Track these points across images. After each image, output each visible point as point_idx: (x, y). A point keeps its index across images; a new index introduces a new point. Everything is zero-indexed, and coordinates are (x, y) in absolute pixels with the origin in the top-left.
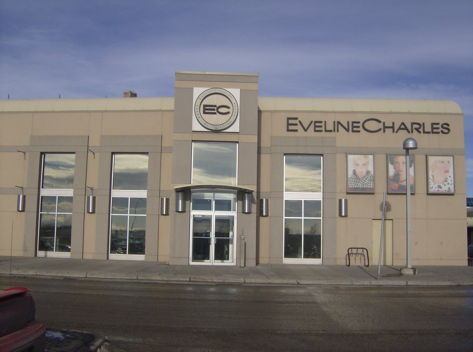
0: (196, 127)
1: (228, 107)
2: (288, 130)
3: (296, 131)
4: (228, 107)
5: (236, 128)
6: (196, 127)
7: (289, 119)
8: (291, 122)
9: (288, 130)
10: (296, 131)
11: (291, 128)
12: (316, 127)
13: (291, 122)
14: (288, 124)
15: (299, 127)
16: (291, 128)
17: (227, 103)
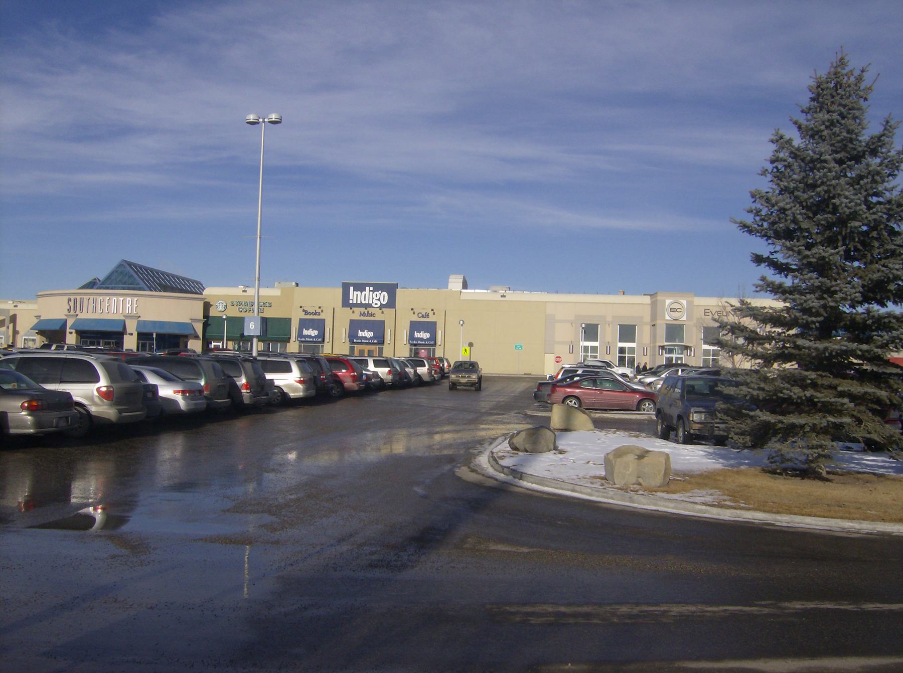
0: (667, 318)
1: (681, 309)
2: (705, 315)
3: (709, 315)
4: (681, 309)
5: (684, 318)
6: (667, 318)
7: (705, 309)
8: (706, 311)
9: (705, 315)
10: (709, 315)
11: (706, 314)
12: (718, 313)
13: (706, 311)
14: (705, 312)
15: (710, 314)
16: (706, 314)
17: (681, 307)
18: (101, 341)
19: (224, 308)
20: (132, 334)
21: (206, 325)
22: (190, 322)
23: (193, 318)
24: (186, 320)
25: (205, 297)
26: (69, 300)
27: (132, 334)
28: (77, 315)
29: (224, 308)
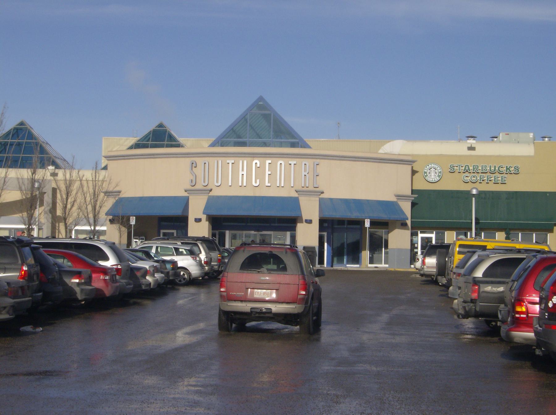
18: (227, 233)
19: (439, 176)
20: (309, 222)
21: (413, 204)
22: (394, 199)
23: (400, 193)
24: (391, 198)
25: (414, 159)
26: (193, 165)
27: (309, 222)
28: (211, 190)
29: (439, 176)
